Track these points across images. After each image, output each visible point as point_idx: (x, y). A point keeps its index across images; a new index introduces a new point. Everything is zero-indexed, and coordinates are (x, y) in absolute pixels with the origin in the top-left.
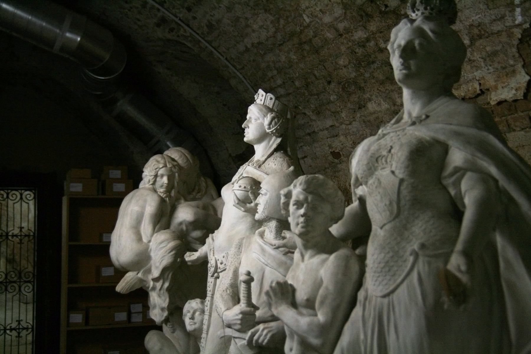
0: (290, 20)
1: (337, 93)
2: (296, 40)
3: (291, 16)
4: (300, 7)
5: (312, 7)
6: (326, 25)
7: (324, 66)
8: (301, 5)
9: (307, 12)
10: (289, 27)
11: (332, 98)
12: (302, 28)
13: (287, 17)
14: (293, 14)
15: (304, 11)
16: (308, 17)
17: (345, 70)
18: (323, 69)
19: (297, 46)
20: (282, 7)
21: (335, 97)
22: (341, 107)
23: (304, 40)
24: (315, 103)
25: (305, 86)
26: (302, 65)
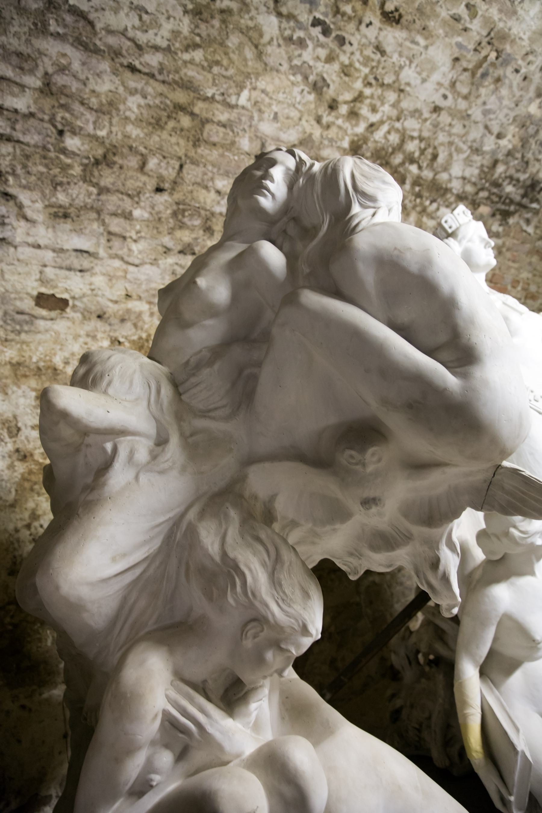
0: (216, 70)
1: (153, 212)
2: (181, 97)
3: (226, 69)
4: (257, 79)
5: (271, 98)
6: (257, 130)
7: (181, 166)
8: (262, 80)
9: (255, 94)
10: (198, 73)
11: (137, 213)
12: (218, 98)
13: (218, 63)
14: (231, 72)
15: (255, 89)
16: (249, 100)
17: (213, 195)
18: (174, 168)
19: (168, 102)
20: (230, 45)
21: (146, 215)
22: (143, 234)
23: (196, 110)
24: (77, 197)
25: (92, 160)
26: (134, 131)
